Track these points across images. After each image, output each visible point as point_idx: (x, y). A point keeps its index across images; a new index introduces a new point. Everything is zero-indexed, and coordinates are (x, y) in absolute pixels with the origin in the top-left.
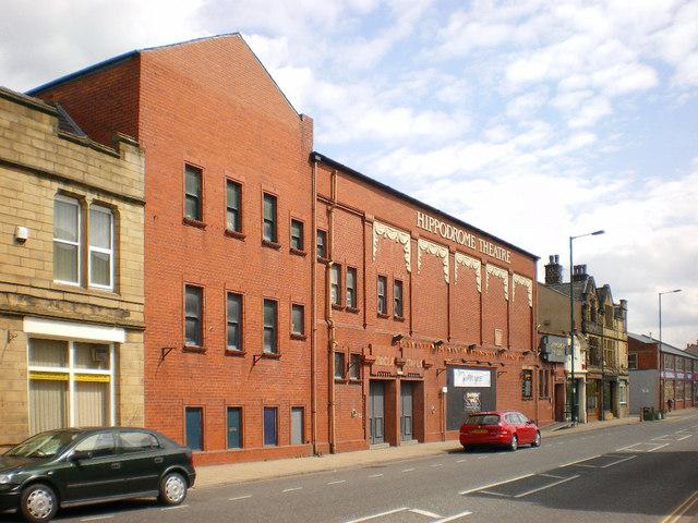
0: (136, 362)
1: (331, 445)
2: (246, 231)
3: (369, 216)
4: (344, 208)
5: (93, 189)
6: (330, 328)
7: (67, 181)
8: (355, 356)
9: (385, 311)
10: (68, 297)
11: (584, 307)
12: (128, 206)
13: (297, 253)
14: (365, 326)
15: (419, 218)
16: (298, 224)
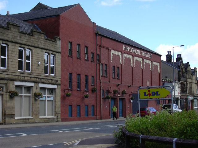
0: (59, 93)
1: (101, 117)
2: (82, 57)
3: (110, 49)
4: (104, 47)
5: (51, 51)
6: (101, 82)
7: (47, 50)
8: (107, 90)
9: (115, 77)
10: (47, 78)
11: (179, 71)
12: (58, 54)
13: (79, 59)
14: (109, 81)
15: (124, 47)
16: (93, 53)
